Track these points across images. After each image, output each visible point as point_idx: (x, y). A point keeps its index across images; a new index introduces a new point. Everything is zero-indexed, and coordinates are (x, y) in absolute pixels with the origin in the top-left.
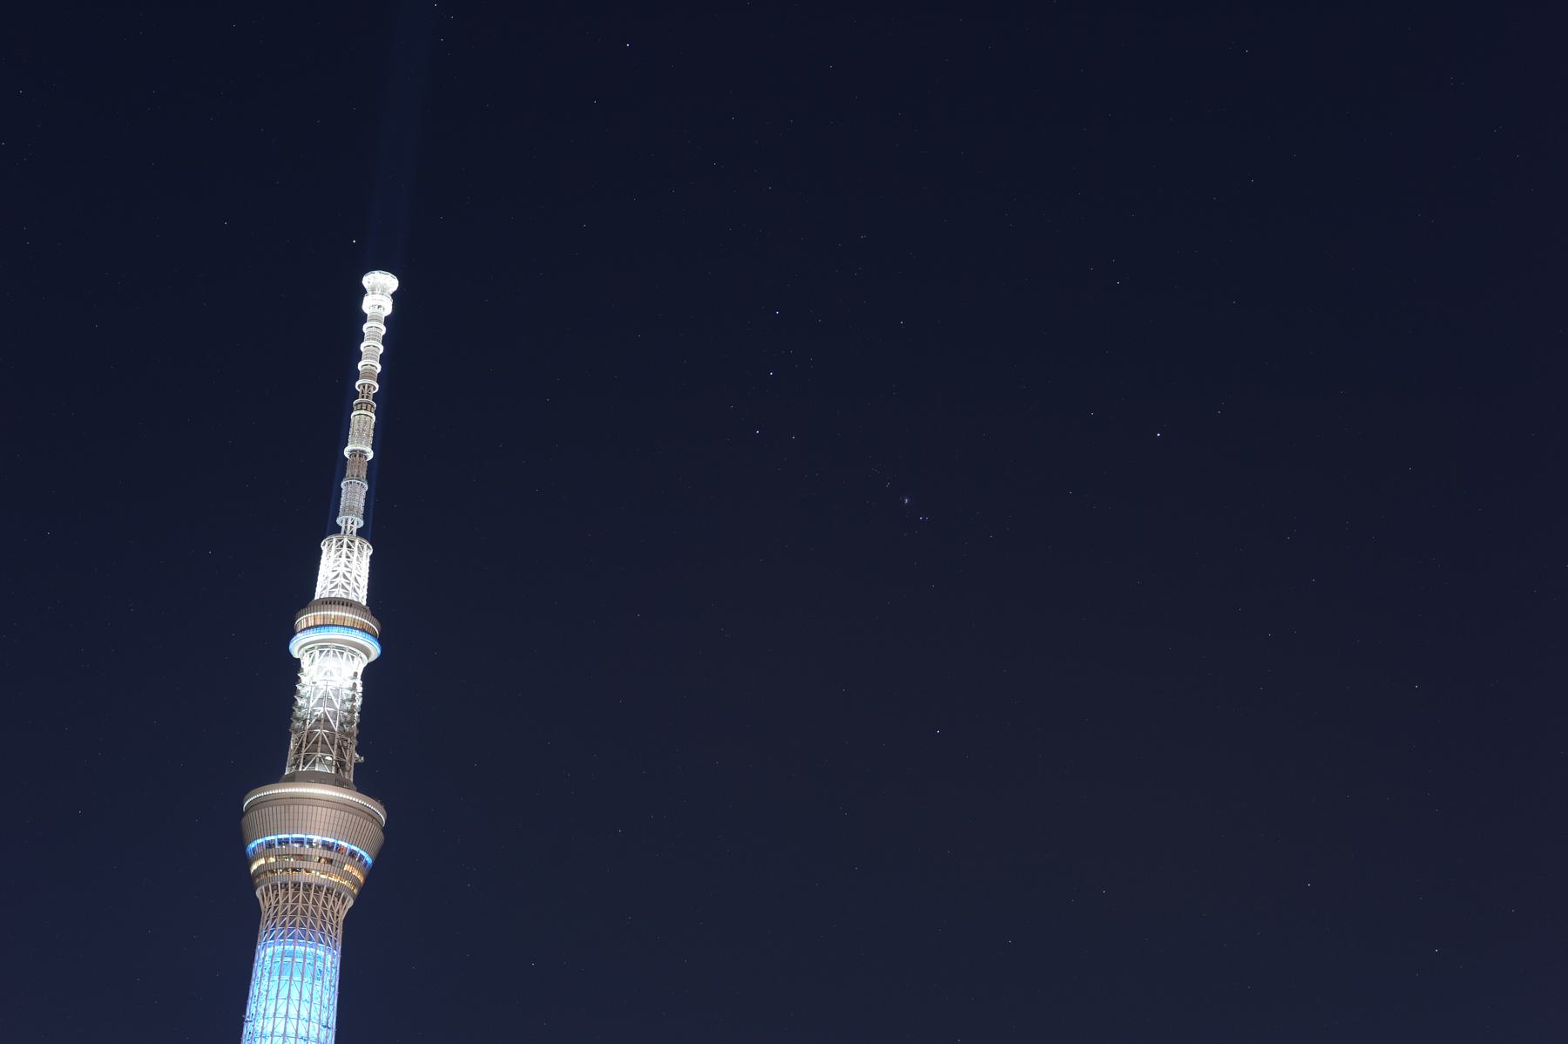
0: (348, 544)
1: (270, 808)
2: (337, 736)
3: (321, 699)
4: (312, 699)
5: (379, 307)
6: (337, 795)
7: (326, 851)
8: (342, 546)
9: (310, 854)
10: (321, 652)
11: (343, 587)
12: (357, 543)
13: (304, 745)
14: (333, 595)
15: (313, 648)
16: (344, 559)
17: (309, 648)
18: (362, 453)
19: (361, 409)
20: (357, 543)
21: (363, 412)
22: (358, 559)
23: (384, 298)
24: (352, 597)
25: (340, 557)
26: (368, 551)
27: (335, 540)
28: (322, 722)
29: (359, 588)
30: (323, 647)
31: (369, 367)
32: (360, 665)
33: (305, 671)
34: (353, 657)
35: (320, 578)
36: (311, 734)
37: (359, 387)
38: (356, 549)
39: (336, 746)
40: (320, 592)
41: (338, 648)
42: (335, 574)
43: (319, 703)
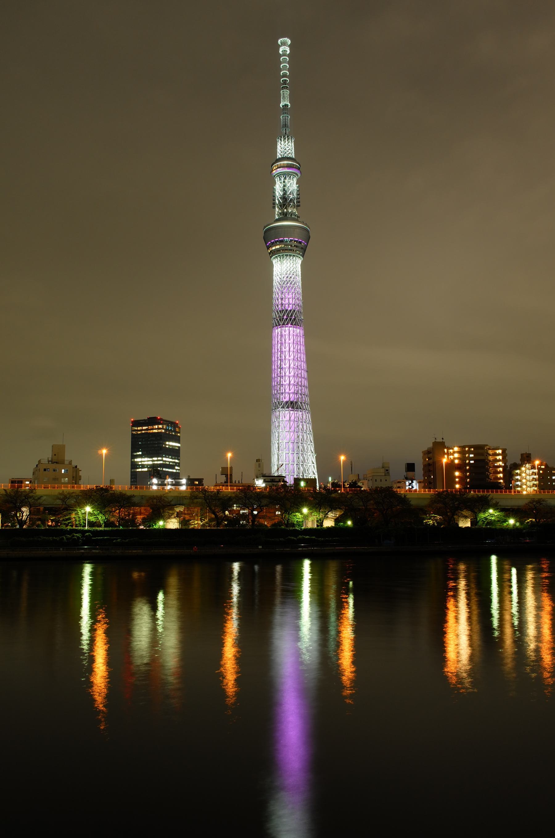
5: (285, 50)
8: (285, 139)
14: (284, 156)
15: (281, 175)
17: (279, 175)
18: (286, 106)
21: (284, 90)
23: (287, 47)
24: (290, 155)
25: (285, 142)
26: (293, 141)
27: (282, 137)
32: (295, 180)
34: (294, 177)
35: (278, 151)
37: (283, 81)
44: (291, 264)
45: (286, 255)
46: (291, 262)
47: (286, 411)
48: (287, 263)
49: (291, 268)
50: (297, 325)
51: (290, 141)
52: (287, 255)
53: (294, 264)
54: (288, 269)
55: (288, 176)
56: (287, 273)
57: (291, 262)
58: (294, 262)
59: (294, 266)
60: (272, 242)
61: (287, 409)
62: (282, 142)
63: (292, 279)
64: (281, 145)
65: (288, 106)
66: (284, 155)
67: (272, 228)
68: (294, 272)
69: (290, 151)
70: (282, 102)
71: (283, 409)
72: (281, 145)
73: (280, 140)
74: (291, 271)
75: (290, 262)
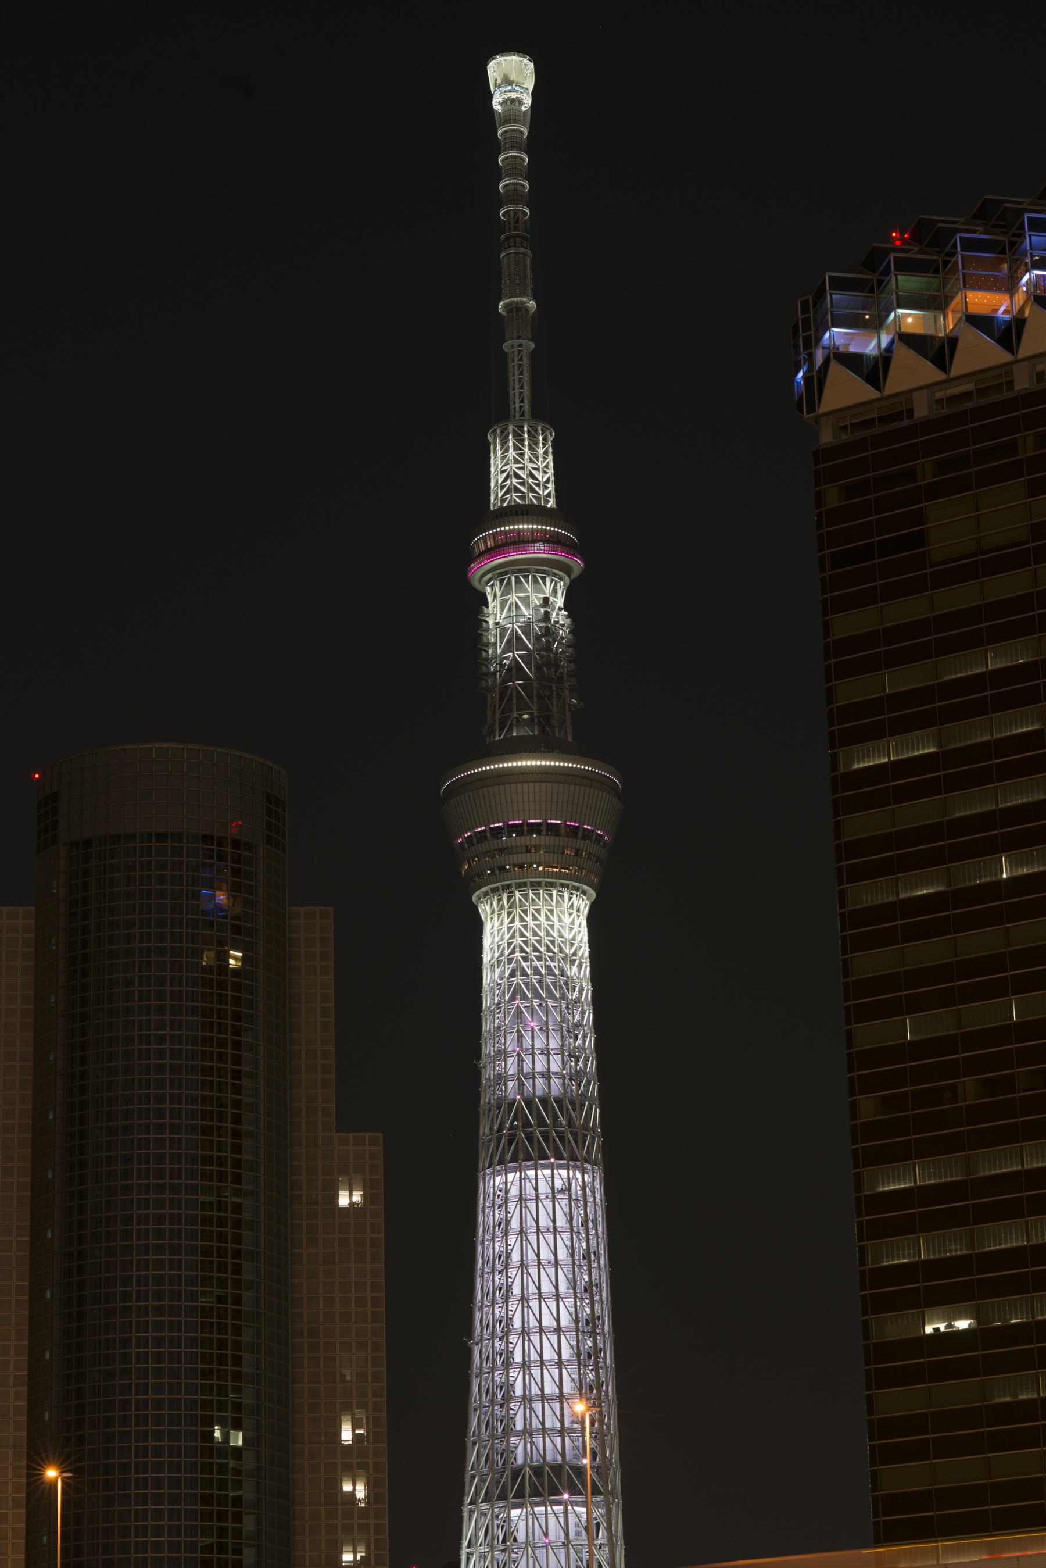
0: (514, 430)
1: (471, 793)
2: (535, 684)
3: (509, 641)
4: (498, 644)
5: (513, 101)
6: (548, 763)
7: (552, 838)
8: (507, 437)
9: (509, 845)
10: (502, 582)
11: (517, 490)
12: (526, 429)
13: (497, 707)
16: (512, 453)
19: (509, 247)
22: (531, 448)
25: (507, 450)
27: (498, 431)
28: (514, 670)
29: (538, 485)
30: (501, 573)
31: (511, 187)
34: (544, 579)
35: (492, 484)
36: (503, 689)
37: (503, 215)
38: (526, 436)
39: (535, 699)
41: (520, 571)
42: (505, 474)
43: (509, 647)
66: (503, 501)
67: (479, 780)
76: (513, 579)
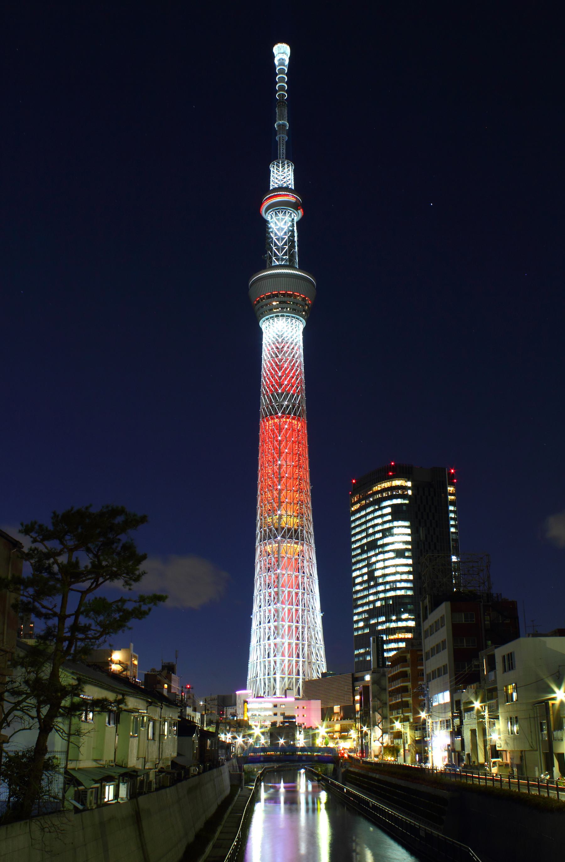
5: (283, 59)
14: (284, 186)
15: (278, 209)
18: (284, 125)
20: (290, 165)
24: (290, 187)
25: (284, 169)
27: (280, 162)
33: (270, 221)
40: (273, 184)
42: (283, 177)
44: (293, 329)
45: (287, 316)
46: (294, 326)
47: (288, 543)
48: (288, 327)
49: (293, 335)
50: (301, 416)
51: (291, 170)
52: (289, 316)
53: (296, 331)
54: (289, 336)
55: (289, 212)
56: (288, 341)
57: (294, 326)
58: (297, 327)
59: (297, 332)
60: (261, 298)
61: (289, 540)
62: (281, 169)
63: (295, 351)
64: (279, 172)
65: (285, 126)
68: (297, 342)
69: (290, 182)
70: (277, 119)
71: (284, 539)
72: (279, 172)
73: (276, 166)
74: (293, 340)
75: (291, 327)
76: (287, 212)
